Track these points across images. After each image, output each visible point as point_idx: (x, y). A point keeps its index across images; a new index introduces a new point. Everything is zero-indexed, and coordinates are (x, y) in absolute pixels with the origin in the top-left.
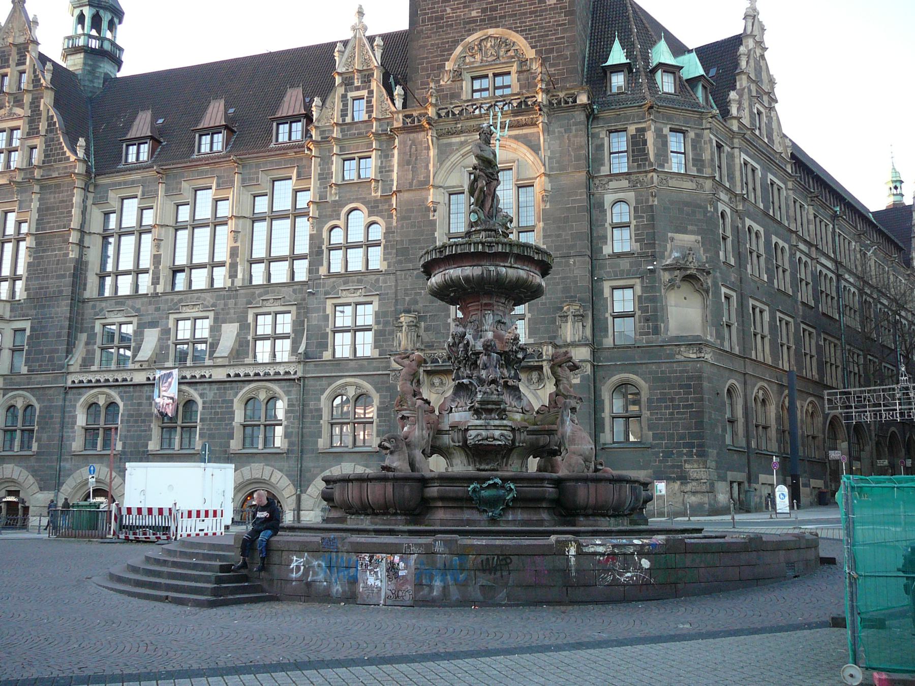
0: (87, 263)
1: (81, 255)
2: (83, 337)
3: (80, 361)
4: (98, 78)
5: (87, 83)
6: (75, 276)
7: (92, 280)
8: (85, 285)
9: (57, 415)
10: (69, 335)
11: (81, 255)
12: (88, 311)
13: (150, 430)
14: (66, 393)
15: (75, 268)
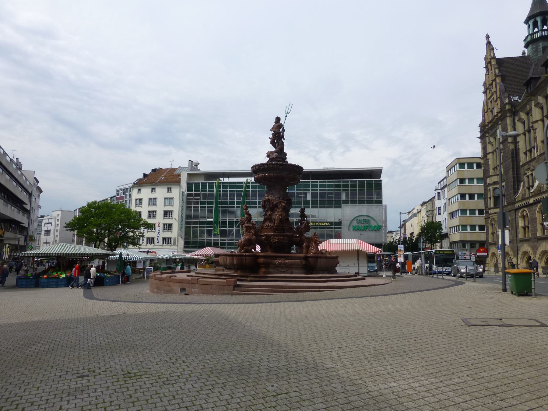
0: (519, 149)
1: (516, 147)
2: (522, 184)
3: (521, 196)
4: (540, 51)
5: (534, 57)
6: (512, 157)
7: (522, 156)
8: (520, 159)
9: (514, 222)
10: (514, 185)
11: (516, 147)
12: (522, 172)
13: (537, 226)
14: (515, 212)
15: (512, 153)
